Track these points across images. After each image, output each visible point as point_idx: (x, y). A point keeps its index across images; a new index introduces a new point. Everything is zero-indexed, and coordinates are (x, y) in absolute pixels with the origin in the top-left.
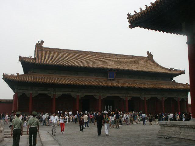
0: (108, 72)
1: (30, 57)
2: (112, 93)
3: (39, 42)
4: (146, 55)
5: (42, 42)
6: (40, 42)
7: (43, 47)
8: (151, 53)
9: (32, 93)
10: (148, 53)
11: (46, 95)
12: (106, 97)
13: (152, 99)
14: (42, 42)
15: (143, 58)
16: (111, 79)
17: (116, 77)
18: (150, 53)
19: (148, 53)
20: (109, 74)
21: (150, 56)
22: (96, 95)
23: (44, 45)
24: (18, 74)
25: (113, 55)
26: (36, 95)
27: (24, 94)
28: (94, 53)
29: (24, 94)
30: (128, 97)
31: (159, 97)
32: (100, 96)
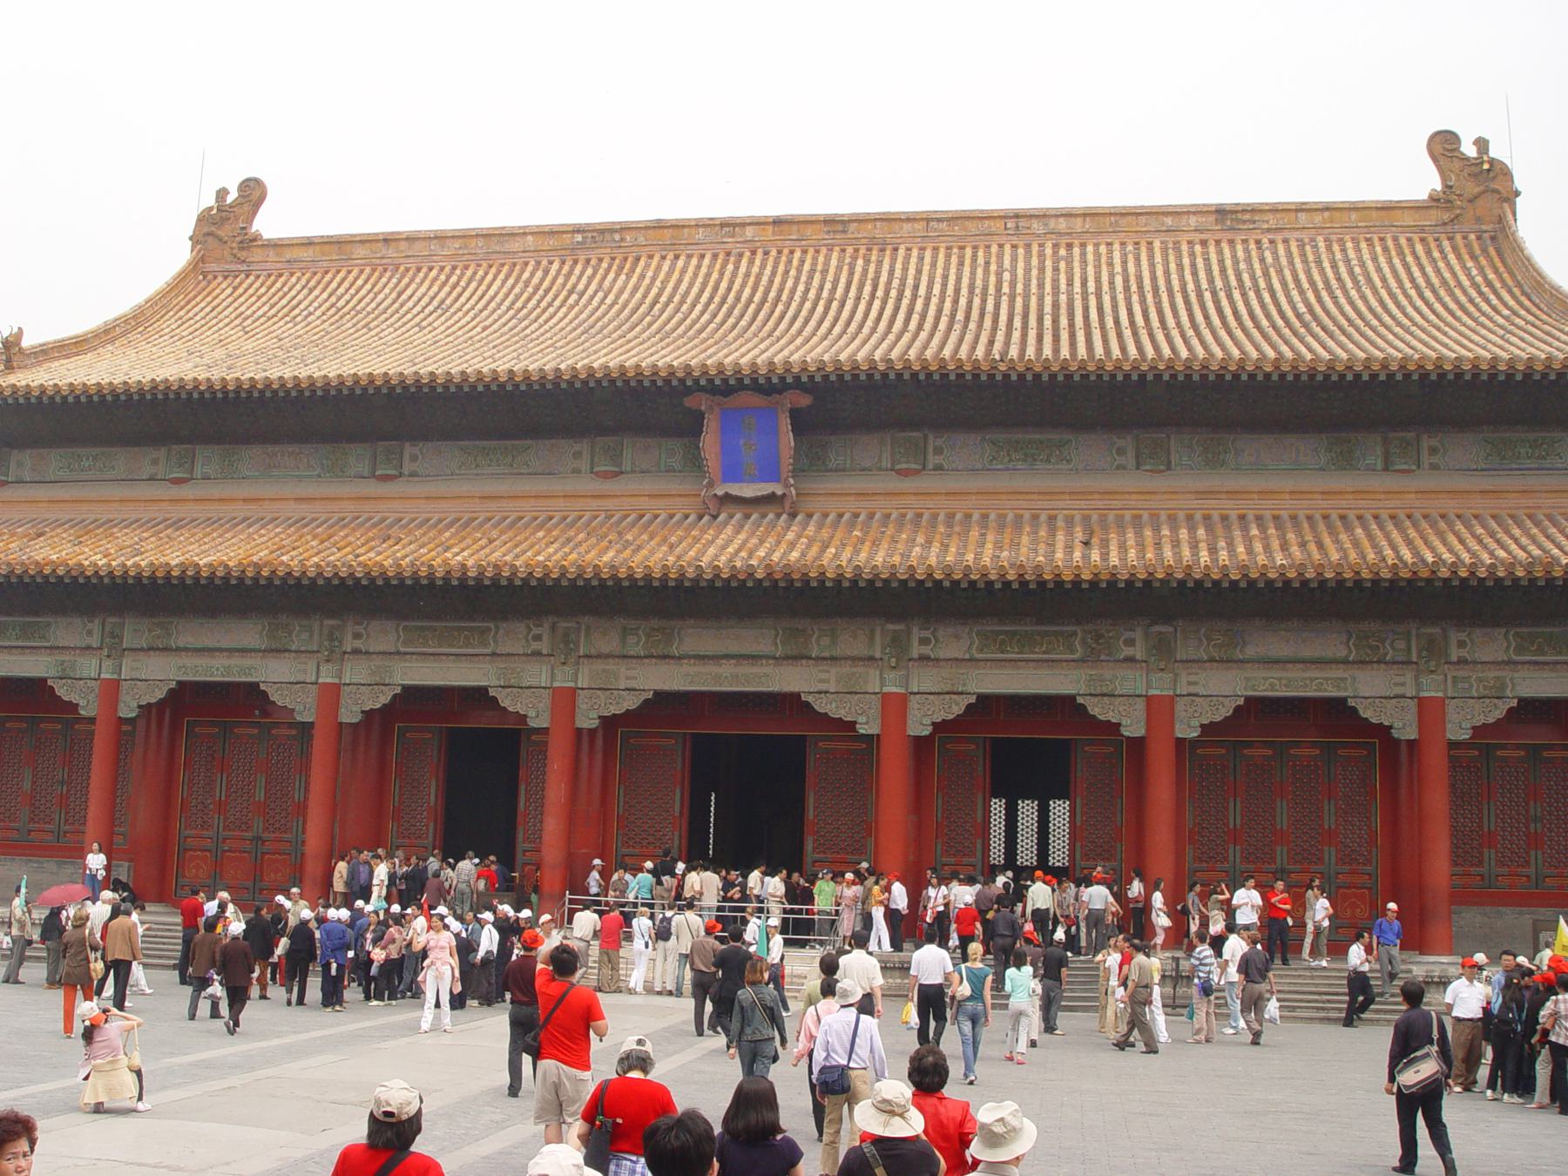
0: (701, 416)
2: (717, 658)
3: (222, 194)
4: (1423, 181)
5: (253, 192)
7: (256, 238)
8: (1482, 144)
10: (1443, 145)
12: (631, 703)
14: (253, 192)
15: (1376, 219)
16: (748, 490)
17: (811, 461)
18: (1469, 150)
19: (1443, 145)
23: (269, 224)
25: (972, 227)
28: (749, 232)
30: (937, 683)
31: (1381, 692)
32: (565, 700)
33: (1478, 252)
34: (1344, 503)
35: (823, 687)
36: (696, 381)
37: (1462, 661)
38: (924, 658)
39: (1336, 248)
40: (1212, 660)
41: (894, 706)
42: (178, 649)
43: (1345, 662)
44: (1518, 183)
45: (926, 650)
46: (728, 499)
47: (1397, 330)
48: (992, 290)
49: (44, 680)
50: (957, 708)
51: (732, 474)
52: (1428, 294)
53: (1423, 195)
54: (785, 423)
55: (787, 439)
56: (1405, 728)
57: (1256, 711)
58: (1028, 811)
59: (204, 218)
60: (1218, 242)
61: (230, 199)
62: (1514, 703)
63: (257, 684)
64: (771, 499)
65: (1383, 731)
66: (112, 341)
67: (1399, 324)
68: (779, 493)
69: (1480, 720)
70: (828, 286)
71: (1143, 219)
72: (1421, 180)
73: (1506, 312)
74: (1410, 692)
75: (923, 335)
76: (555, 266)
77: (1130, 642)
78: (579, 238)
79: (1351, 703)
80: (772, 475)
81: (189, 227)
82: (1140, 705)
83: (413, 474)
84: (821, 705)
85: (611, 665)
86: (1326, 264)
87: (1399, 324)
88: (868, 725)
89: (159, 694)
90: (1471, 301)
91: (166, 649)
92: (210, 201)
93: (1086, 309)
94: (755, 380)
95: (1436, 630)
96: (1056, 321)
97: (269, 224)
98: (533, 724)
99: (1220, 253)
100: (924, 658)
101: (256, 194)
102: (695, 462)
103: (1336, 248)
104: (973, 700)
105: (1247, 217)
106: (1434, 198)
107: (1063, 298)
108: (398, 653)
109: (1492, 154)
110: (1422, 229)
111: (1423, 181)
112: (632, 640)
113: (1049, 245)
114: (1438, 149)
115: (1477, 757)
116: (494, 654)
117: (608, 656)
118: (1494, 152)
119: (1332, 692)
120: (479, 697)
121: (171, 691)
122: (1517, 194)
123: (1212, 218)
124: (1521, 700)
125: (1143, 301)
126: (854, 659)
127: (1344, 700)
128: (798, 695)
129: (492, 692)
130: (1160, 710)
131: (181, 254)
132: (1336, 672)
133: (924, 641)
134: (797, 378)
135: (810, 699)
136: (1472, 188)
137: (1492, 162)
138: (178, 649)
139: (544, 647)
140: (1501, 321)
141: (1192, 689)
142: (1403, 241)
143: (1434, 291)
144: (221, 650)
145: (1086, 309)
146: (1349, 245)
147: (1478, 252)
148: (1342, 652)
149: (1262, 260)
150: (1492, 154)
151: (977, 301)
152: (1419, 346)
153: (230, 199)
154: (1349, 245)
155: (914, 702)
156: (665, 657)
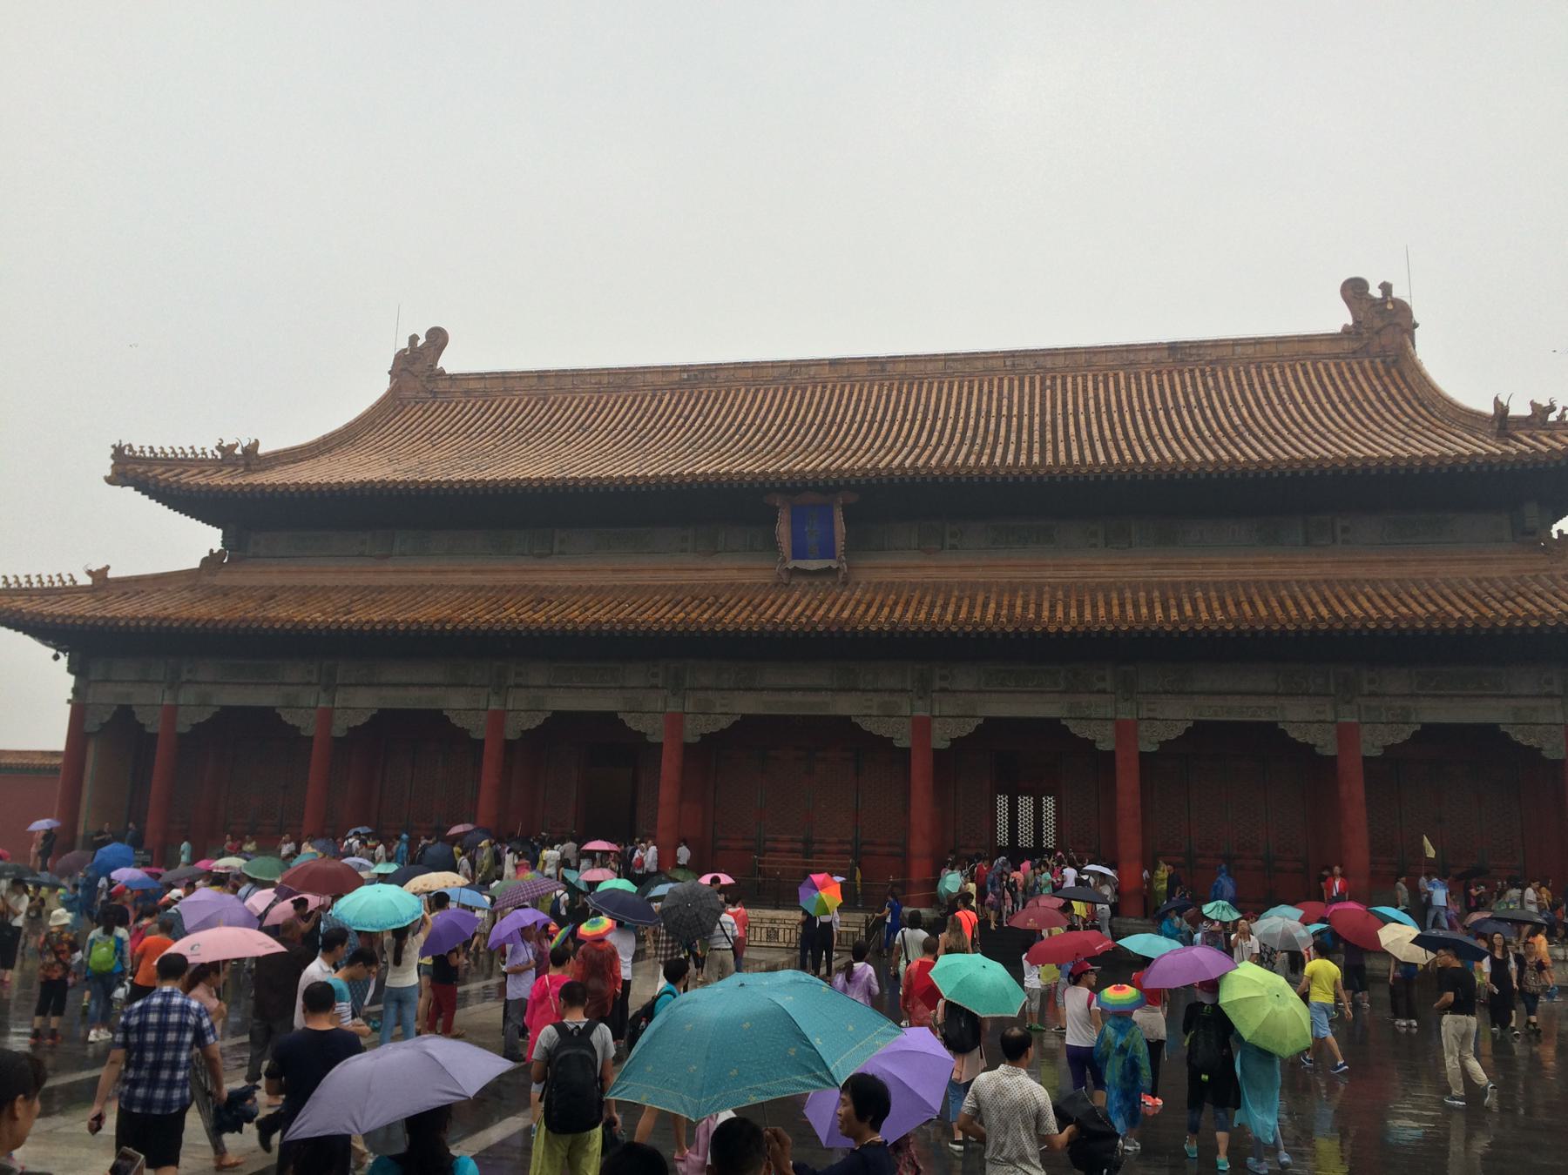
0: (776, 510)
1: (219, 448)
3: (414, 339)
5: (438, 338)
7: (442, 372)
8: (1386, 288)
9: (175, 702)
10: (1354, 290)
11: (267, 715)
12: (725, 723)
13: (1205, 739)
14: (438, 338)
16: (814, 565)
17: (859, 543)
18: (1375, 292)
19: (1354, 290)
20: (783, 531)
21: (1381, 324)
22: (650, 709)
23: (451, 362)
24: (99, 576)
26: (205, 715)
27: (125, 713)
29: (125, 713)
31: (1304, 718)
33: (1382, 372)
34: (1272, 571)
35: (869, 712)
36: (773, 484)
37: (1372, 694)
38: (943, 690)
39: (1265, 373)
40: (1166, 692)
41: (922, 727)
43: (1276, 694)
44: (1417, 317)
45: (945, 684)
46: (796, 571)
47: (1316, 436)
48: (994, 413)
49: (273, 708)
50: (969, 727)
51: (798, 553)
52: (1341, 407)
54: (839, 516)
55: (840, 528)
56: (1327, 744)
57: (1199, 729)
58: (1025, 804)
59: (400, 357)
60: (1170, 373)
61: (420, 343)
62: (1418, 728)
63: (441, 711)
64: (828, 571)
65: (1308, 748)
66: (329, 451)
67: (1317, 431)
68: (835, 567)
69: (1391, 741)
70: (870, 411)
71: (1110, 356)
72: (1335, 318)
73: (1406, 420)
74: (1330, 717)
75: (942, 449)
76: (667, 398)
77: (1103, 679)
78: (685, 376)
79: (1281, 726)
80: (828, 553)
82: (1110, 727)
83: (561, 553)
84: (867, 725)
86: (1257, 386)
87: (1317, 431)
88: (902, 742)
89: (363, 719)
90: (1377, 412)
91: (370, 685)
93: (1066, 426)
94: (816, 483)
96: (1042, 436)
97: (451, 362)
98: (651, 739)
99: (1171, 380)
100: (943, 690)
101: (440, 341)
102: (772, 545)
103: (1265, 373)
104: (981, 721)
105: (1194, 351)
106: (1346, 330)
107: (1048, 417)
108: (550, 687)
109: (1395, 294)
110: (1336, 356)
111: (1335, 318)
113: (1038, 378)
114: (1350, 292)
115: (1386, 771)
116: (621, 688)
117: (707, 689)
119: (1265, 718)
120: (610, 718)
121: (373, 717)
122: (1416, 326)
123: (1166, 353)
124: (1424, 725)
125: (1110, 420)
126: (892, 691)
127: (1275, 724)
128: (848, 718)
129: (620, 716)
130: (1125, 730)
131: (380, 385)
132: (1269, 702)
133: (944, 678)
134: (847, 482)
135: (858, 721)
136: (1378, 323)
137: (1397, 302)
140: (1402, 427)
141: (1151, 715)
142: (1320, 366)
143: (1346, 404)
144: (413, 685)
145: (1066, 426)
146: (1276, 370)
147: (1382, 372)
149: (1205, 384)
150: (1395, 294)
151: (982, 421)
152: (1334, 449)
153: (420, 343)
154: (1276, 370)
155: (936, 724)
156: (750, 689)
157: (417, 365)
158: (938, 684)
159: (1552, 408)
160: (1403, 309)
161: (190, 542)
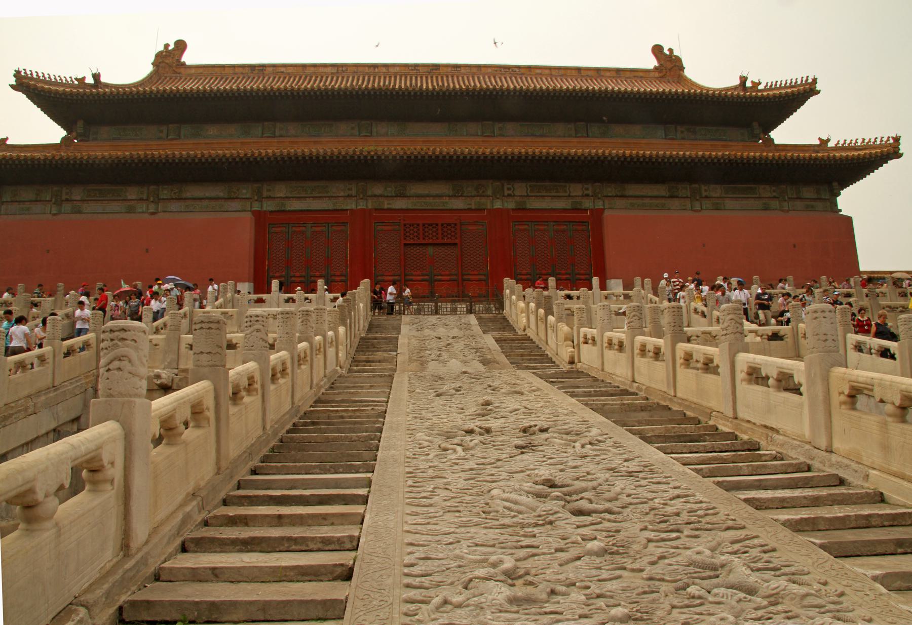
3: (167, 46)
5: (181, 46)
6: (171, 47)
7: (184, 64)
8: (671, 50)
10: (657, 50)
14: (181, 46)
19: (657, 50)
23: (189, 58)
40: (617, 196)
42: (185, 199)
45: (510, 192)
53: (652, 67)
59: (159, 55)
61: (170, 48)
81: (152, 59)
85: (381, 199)
92: (162, 48)
95: (697, 186)
97: (189, 58)
100: (509, 195)
106: (656, 68)
112: (389, 189)
118: (675, 53)
133: (509, 189)
136: (669, 65)
138: (185, 199)
139: (354, 193)
148: (664, 194)
153: (170, 48)
157: (169, 59)
158: (506, 192)
159: (760, 83)
160: (678, 60)
161: (51, 133)
